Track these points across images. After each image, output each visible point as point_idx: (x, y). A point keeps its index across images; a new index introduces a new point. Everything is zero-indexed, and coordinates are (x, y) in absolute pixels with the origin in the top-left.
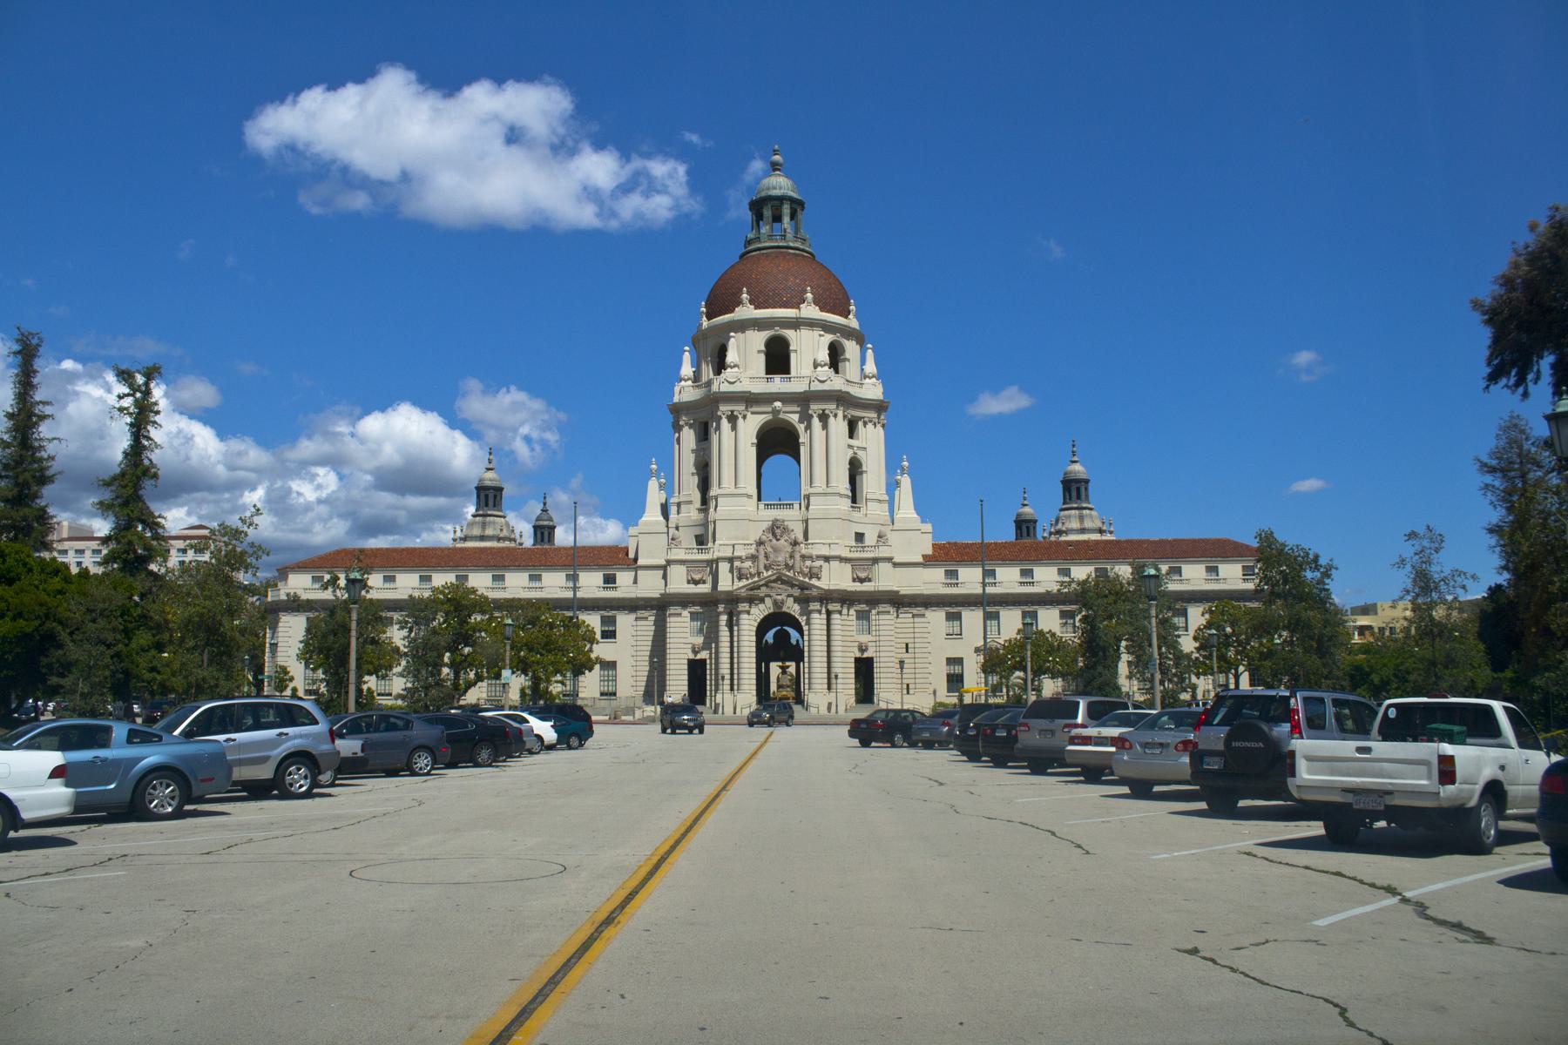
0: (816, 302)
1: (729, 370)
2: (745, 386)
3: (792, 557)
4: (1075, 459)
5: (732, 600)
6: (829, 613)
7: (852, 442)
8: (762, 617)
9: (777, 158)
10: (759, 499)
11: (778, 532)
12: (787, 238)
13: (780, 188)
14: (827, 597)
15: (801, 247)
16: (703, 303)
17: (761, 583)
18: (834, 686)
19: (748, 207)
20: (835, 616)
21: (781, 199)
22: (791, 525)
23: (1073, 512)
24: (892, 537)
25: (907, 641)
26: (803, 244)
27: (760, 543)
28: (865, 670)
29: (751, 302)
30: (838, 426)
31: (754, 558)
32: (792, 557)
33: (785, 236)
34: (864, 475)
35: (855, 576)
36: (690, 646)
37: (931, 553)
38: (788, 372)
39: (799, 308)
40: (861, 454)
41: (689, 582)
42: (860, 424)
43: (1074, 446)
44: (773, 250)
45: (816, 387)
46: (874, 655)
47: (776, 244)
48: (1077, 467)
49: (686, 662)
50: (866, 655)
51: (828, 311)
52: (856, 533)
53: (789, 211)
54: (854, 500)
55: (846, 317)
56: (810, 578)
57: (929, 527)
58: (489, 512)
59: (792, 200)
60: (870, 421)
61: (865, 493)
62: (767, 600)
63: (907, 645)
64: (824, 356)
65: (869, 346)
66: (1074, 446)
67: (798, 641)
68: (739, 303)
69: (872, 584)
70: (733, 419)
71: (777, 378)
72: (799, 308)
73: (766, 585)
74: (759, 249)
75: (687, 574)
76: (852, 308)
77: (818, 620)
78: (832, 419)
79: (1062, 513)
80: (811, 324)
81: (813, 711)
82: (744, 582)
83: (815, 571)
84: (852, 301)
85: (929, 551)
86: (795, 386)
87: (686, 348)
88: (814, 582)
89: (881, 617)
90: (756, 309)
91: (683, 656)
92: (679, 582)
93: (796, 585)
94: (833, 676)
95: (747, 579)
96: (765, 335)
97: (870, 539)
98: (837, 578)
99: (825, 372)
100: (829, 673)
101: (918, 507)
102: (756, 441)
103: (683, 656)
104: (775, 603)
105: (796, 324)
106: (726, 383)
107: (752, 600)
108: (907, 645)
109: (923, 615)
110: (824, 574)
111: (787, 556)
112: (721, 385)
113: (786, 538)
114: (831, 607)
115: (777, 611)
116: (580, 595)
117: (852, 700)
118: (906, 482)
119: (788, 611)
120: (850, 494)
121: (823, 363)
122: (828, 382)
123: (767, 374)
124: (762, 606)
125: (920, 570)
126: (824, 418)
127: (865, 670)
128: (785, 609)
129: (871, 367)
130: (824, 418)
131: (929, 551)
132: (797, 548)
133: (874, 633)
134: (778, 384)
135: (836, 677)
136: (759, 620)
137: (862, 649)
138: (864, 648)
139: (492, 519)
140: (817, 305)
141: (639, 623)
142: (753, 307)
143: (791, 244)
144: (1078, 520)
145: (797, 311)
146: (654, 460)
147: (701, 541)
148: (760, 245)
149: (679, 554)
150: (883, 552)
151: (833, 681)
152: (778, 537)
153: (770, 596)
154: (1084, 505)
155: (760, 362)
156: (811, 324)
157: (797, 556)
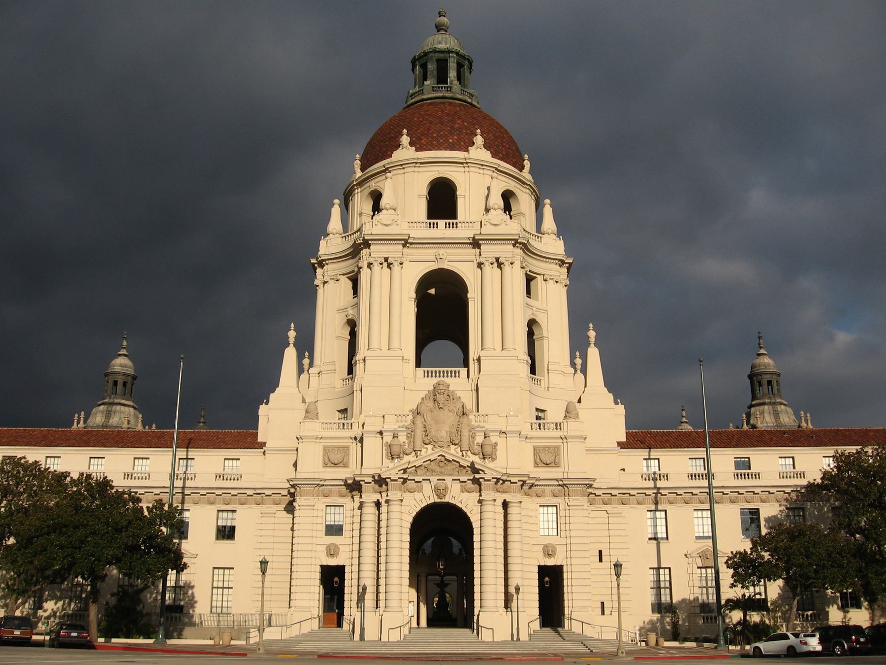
0: (487, 146)
1: (384, 212)
2: (401, 229)
3: (459, 431)
4: (762, 351)
5: (381, 481)
6: (505, 505)
8: (418, 509)
9: (444, 20)
10: (418, 364)
11: (441, 398)
12: (453, 90)
13: (446, 43)
15: (469, 100)
16: (358, 156)
18: (514, 604)
21: (449, 51)
22: (459, 394)
23: (766, 407)
26: (470, 98)
27: (417, 412)
33: (451, 87)
34: (545, 342)
35: (538, 460)
36: (324, 548)
37: (625, 440)
38: (454, 215)
39: (467, 151)
40: (540, 318)
41: (325, 465)
43: (760, 338)
44: (437, 100)
45: (488, 230)
46: (564, 563)
47: (441, 95)
48: (766, 360)
49: (318, 569)
50: (550, 562)
51: (501, 159)
53: (455, 65)
54: (533, 371)
55: (521, 171)
57: (623, 406)
58: (116, 401)
59: (457, 54)
60: (552, 279)
61: (546, 364)
62: (426, 486)
63: (600, 552)
65: (547, 201)
66: (760, 338)
67: (460, 550)
68: (398, 146)
69: (560, 470)
71: (441, 223)
72: (467, 151)
74: (423, 100)
75: (324, 455)
76: (527, 164)
77: (494, 513)
78: (507, 268)
79: (753, 409)
81: (486, 636)
83: (488, 450)
84: (526, 156)
85: (623, 439)
86: (463, 232)
87: (337, 201)
88: (488, 463)
90: (417, 151)
91: (313, 561)
93: (464, 467)
95: (399, 457)
97: (555, 414)
99: (498, 215)
100: (506, 586)
101: (611, 383)
102: (415, 296)
103: (313, 561)
104: (437, 490)
106: (380, 226)
108: (600, 552)
110: (500, 453)
111: (454, 430)
113: (452, 408)
114: (508, 497)
115: (439, 500)
117: (536, 625)
118: (593, 354)
120: (530, 362)
121: (496, 207)
122: (503, 225)
123: (428, 219)
124: (418, 495)
128: (447, 499)
129: (549, 223)
131: (623, 439)
133: (563, 534)
134: (442, 230)
135: (517, 589)
136: (414, 514)
137: (548, 552)
138: (550, 553)
139: (118, 407)
140: (488, 150)
141: (264, 520)
142: (414, 148)
143: (459, 96)
144: (772, 416)
145: (466, 153)
146: (292, 325)
148: (425, 97)
152: (441, 406)
154: (779, 400)
155: (421, 207)
157: (466, 433)
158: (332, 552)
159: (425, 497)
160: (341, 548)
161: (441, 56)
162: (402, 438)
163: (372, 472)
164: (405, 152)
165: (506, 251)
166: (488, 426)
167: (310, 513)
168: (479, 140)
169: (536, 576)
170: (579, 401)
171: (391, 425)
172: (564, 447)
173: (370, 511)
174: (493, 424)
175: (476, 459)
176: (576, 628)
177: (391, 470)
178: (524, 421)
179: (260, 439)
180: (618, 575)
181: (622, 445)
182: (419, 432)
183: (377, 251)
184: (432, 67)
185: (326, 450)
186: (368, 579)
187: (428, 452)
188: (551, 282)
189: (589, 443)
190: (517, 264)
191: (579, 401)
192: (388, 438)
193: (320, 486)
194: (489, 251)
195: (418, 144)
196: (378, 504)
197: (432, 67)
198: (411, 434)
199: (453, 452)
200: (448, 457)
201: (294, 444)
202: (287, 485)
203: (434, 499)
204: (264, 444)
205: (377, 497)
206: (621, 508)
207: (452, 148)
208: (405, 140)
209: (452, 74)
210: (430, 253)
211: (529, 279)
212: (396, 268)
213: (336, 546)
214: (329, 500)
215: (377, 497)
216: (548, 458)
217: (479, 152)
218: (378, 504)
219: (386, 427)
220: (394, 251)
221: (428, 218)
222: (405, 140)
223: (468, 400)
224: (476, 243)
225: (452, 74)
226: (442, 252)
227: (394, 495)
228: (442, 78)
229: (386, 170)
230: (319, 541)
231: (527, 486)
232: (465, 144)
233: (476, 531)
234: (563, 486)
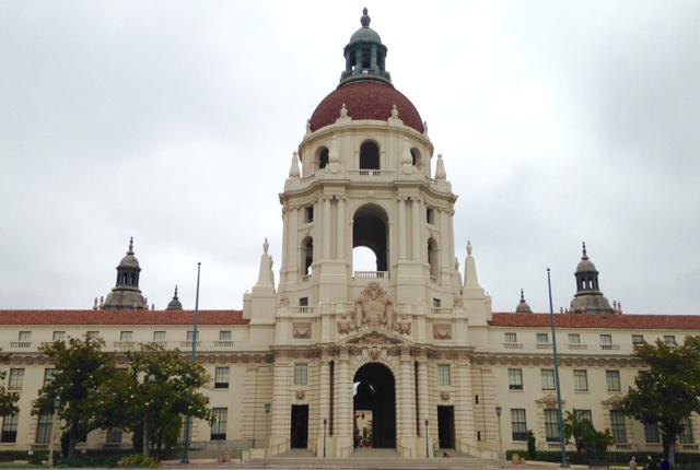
3: (385, 315)
5: (335, 351)
6: (416, 364)
7: (430, 226)
14: (414, 351)
17: (360, 336)
18: (423, 432)
19: (343, 52)
20: (422, 368)
22: (385, 290)
24: (465, 304)
25: (477, 393)
28: (446, 416)
29: (349, 114)
30: (419, 211)
31: (353, 316)
32: (385, 315)
36: (294, 393)
38: (378, 168)
39: (386, 120)
40: (436, 237)
41: (295, 336)
42: (435, 210)
50: (446, 404)
51: (409, 125)
52: (435, 299)
56: (402, 333)
62: (365, 352)
64: (408, 156)
68: (339, 116)
70: (334, 200)
71: (371, 172)
72: (386, 120)
73: (363, 338)
77: (408, 370)
78: (415, 205)
80: (397, 131)
81: (406, 454)
82: (345, 336)
83: (405, 327)
89: (460, 370)
92: (284, 337)
94: (422, 422)
95: (347, 332)
96: (360, 138)
97: (446, 303)
98: (421, 335)
99: (409, 167)
100: (418, 419)
104: (372, 353)
105: (385, 131)
107: (351, 352)
108: (477, 397)
109: (489, 371)
111: (382, 314)
112: (324, 175)
116: (197, 349)
119: (382, 362)
124: (359, 357)
125: (485, 332)
126: (409, 201)
127: (446, 416)
128: (379, 360)
130: (409, 201)
132: (389, 307)
137: (444, 397)
141: (250, 373)
147: (304, 301)
149: (284, 312)
150: (459, 313)
151: (423, 426)
153: (367, 348)
156: (397, 131)
157: (390, 315)
158: (301, 396)
159: (362, 359)
160: (307, 393)
161: (365, 46)
162: (349, 319)
163: (328, 342)
164: (344, 121)
165: (414, 193)
166: (405, 312)
167: (285, 369)
168: (395, 112)
169: (436, 413)
170: (461, 293)
171: (340, 310)
172: (454, 325)
173: (325, 369)
174: (408, 310)
175: (395, 333)
176: (464, 449)
177: (341, 340)
178: (424, 309)
179: (244, 317)
180: (499, 415)
181: (489, 322)
182: (359, 315)
183: (329, 192)
184: (359, 54)
185: (295, 326)
186: (325, 414)
187: (366, 329)
188: (443, 213)
189: (470, 323)
190: (422, 201)
191: (461, 293)
192: (338, 319)
193: (292, 352)
194: (404, 193)
195: (354, 115)
196: (332, 364)
197: (359, 54)
198: (353, 316)
199: (381, 330)
200: (380, 332)
201: (272, 321)
202: (268, 349)
203: (370, 360)
204: (249, 320)
205: (330, 359)
206: (490, 367)
207: (377, 118)
208: (344, 111)
209: (374, 60)
210: (362, 193)
211: (429, 212)
212: (341, 204)
213: (303, 393)
214: (297, 361)
215: (330, 359)
216: (443, 333)
217: (395, 122)
218: (332, 364)
219: (338, 311)
220: (340, 192)
221: (362, 166)
222: (344, 111)
223: (389, 294)
224: (394, 187)
225: (374, 60)
226: (371, 192)
227: (344, 356)
228: (366, 65)
229: (331, 133)
230: (292, 388)
231: (432, 354)
232: (385, 116)
233: (397, 382)
234: (454, 354)
